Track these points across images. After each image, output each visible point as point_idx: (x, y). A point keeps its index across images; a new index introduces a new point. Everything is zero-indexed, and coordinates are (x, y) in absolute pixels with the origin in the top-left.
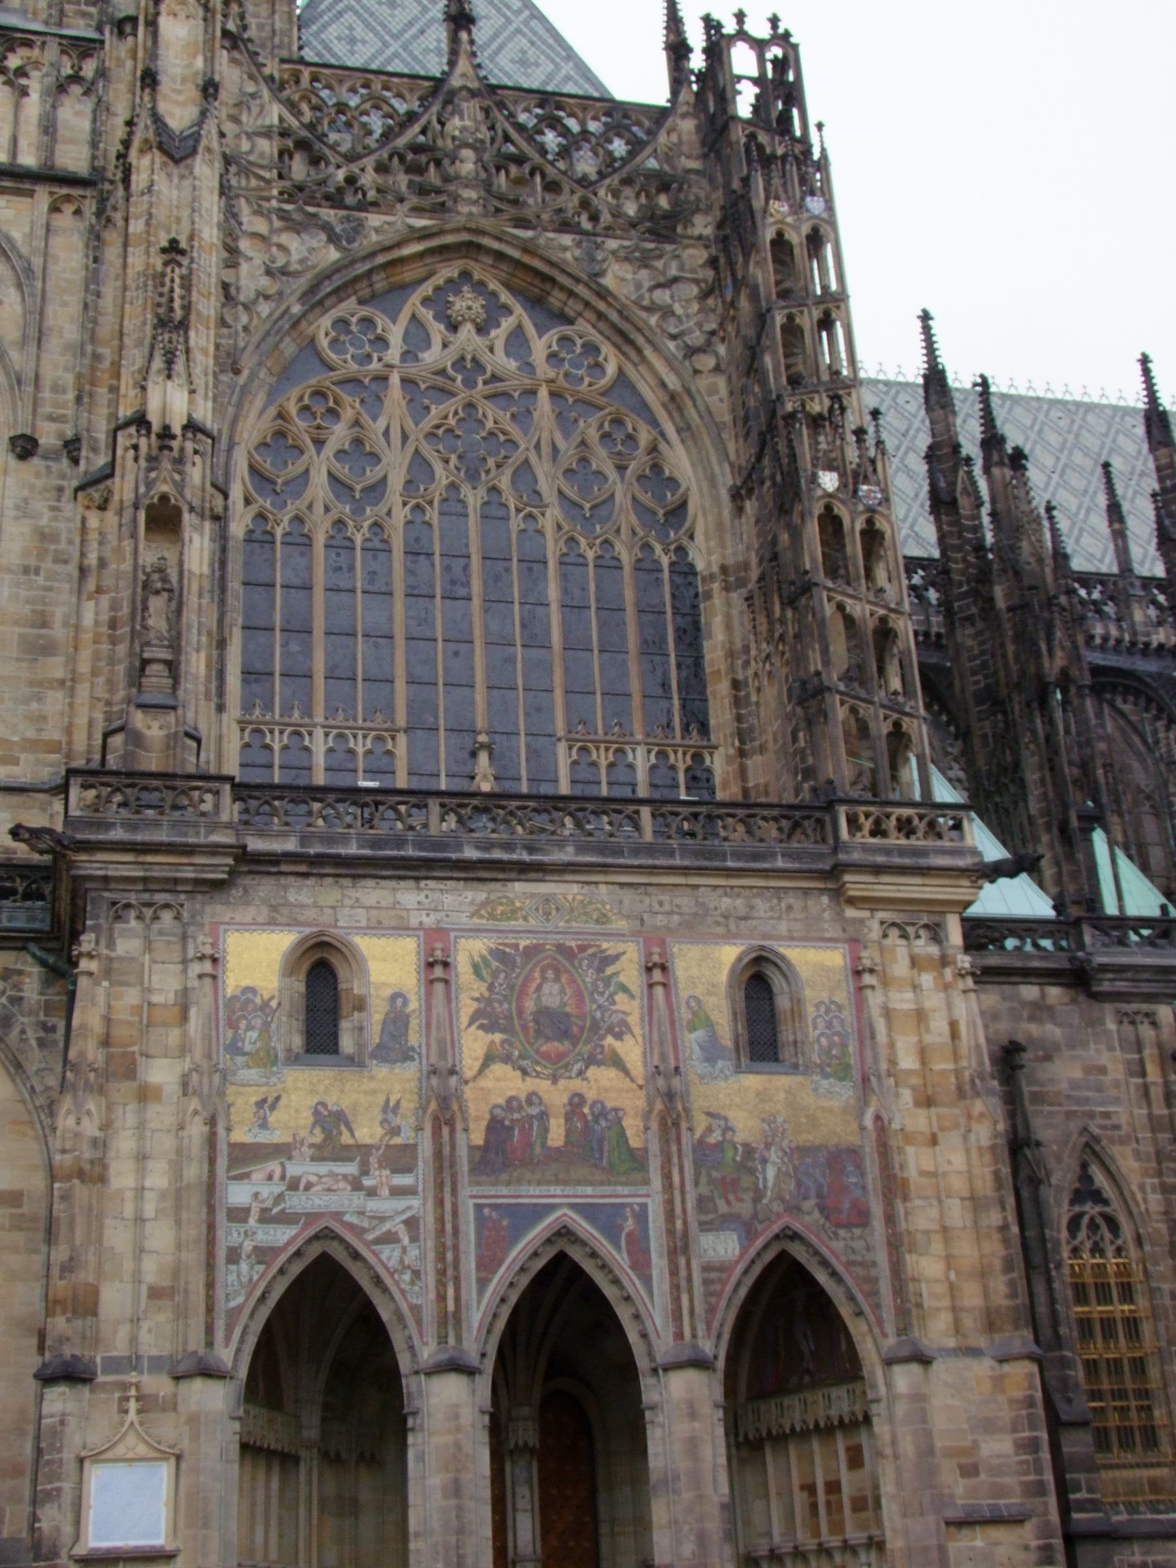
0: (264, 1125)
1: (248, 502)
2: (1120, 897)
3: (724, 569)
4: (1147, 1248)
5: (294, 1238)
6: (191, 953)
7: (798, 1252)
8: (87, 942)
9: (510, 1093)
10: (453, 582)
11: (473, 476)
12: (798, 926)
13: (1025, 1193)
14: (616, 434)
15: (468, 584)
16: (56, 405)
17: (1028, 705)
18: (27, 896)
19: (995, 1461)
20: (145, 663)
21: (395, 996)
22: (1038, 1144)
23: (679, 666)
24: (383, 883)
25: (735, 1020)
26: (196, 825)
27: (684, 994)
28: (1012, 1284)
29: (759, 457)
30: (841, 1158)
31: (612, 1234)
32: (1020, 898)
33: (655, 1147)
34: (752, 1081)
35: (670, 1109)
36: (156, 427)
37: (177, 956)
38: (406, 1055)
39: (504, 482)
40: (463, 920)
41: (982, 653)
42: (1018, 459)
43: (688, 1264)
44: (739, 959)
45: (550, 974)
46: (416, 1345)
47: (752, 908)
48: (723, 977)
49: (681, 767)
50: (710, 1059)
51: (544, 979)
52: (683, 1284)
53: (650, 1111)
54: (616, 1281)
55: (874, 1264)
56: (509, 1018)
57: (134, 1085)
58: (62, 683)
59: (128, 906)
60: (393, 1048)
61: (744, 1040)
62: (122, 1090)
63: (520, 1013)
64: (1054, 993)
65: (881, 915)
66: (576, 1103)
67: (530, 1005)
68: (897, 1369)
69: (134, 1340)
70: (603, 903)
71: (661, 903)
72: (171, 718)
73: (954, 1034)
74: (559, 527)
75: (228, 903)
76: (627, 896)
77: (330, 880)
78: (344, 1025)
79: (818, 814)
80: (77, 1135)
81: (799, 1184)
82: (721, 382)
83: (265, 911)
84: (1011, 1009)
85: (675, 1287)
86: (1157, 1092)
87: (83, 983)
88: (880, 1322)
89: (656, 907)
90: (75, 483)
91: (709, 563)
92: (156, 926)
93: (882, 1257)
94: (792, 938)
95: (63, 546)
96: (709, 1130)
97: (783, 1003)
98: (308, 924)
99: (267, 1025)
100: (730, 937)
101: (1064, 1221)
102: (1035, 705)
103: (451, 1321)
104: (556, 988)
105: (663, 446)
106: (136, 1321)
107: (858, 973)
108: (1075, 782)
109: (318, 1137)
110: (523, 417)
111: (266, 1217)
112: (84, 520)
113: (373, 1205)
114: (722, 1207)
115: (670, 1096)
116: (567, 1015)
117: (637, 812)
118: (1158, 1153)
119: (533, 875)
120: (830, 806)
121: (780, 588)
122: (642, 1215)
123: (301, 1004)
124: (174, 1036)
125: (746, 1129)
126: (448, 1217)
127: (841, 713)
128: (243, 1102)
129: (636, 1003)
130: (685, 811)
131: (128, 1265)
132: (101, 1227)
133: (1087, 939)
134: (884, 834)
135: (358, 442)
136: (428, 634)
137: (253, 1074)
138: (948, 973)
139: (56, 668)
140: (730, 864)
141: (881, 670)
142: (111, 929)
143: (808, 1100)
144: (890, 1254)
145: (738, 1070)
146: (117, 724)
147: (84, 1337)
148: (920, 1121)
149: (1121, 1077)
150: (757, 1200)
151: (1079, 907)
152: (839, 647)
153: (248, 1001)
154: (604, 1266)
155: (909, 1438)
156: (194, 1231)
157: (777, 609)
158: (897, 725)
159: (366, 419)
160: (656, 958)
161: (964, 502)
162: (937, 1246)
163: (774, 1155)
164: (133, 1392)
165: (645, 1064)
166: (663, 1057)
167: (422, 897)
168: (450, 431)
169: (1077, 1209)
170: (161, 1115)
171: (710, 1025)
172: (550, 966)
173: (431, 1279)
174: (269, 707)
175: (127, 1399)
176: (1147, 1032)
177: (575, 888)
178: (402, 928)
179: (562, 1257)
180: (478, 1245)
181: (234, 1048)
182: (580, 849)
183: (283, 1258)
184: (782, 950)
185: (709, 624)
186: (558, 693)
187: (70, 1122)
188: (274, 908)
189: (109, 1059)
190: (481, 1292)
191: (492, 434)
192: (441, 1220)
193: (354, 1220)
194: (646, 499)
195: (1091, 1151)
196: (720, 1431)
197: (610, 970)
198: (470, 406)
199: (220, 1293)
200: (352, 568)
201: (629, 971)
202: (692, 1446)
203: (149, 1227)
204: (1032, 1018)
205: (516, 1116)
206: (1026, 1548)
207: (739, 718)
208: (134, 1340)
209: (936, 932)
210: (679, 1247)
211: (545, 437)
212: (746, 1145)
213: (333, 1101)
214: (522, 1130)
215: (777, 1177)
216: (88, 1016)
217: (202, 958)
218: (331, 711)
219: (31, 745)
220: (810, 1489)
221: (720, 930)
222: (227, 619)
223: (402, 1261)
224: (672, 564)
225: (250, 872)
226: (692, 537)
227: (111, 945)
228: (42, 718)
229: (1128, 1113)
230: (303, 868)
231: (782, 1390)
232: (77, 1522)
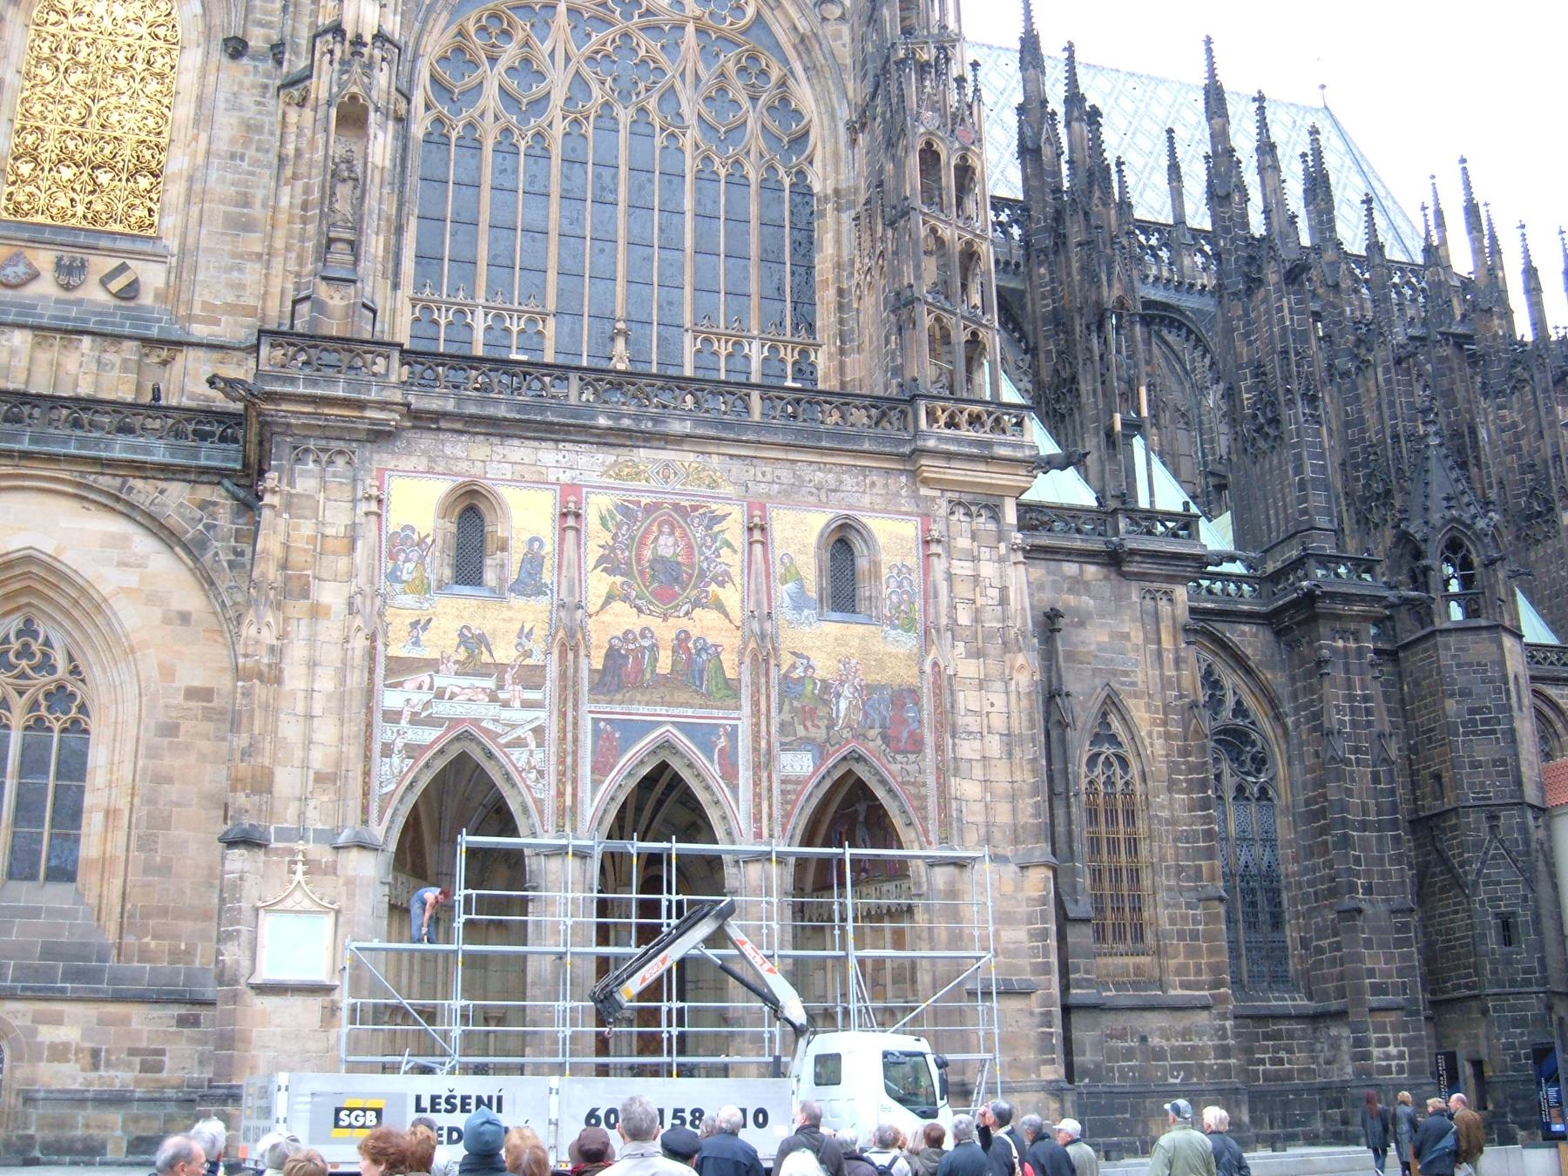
0: (416, 643)
1: (428, 108)
2: (1152, 494)
3: (837, 192)
4: (1150, 783)
5: (439, 738)
6: (360, 494)
7: (862, 772)
8: (271, 479)
10: (603, 189)
11: (625, 96)
12: (879, 500)
13: (1054, 734)
14: (751, 67)
15: (615, 191)
16: (265, 12)
17: (1088, 328)
18: (223, 439)
19: (1012, 946)
20: (331, 241)
22: (1068, 695)
23: (793, 273)
24: (527, 443)
25: (821, 576)
26: (369, 384)
27: (779, 552)
28: (1037, 805)
29: (873, 97)
30: (904, 697)
31: (707, 749)
32: (1067, 489)
33: (746, 678)
35: (762, 651)
36: (350, 35)
37: (347, 495)
38: (539, 590)
39: (652, 104)
40: (595, 479)
41: (1052, 280)
42: (1094, 116)
43: (770, 777)
44: (828, 525)
45: (666, 529)
47: (841, 482)
48: (813, 540)
49: (790, 360)
50: (798, 608)
51: (661, 532)
52: (764, 793)
53: (745, 648)
54: (708, 788)
55: (924, 784)
56: (629, 564)
57: (308, 602)
58: (260, 256)
59: (307, 450)
60: (528, 584)
61: (828, 591)
62: (297, 607)
63: (639, 561)
64: (1091, 570)
65: (949, 494)
66: (682, 638)
67: (648, 554)
68: (937, 870)
69: (301, 815)
71: (764, 474)
72: (351, 290)
73: (1003, 601)
74: (697, 147)
75: (393, 453)
76: (736, 466)
77: (482, 438)
78: (488, 561)
79: (902, 407)
80: (257, 642)
81: (866, 715)
82: (845, 30)
83: (424, 461)
84: (1054, 582)
85: (757, 795)
86: (1169, 657)
87: (267, 514)
88: (926, 832)
89: (759, 477)
90: (278, 82)
91: (825, 187)
93: (931, 780)
94: (874, 510)
95: (265, 137)
96: (794, 666)
97: (862, 564)
99: (422, 558)
100: (821, 505)
101: (1085, 759)
102: (1093, 327)
103: (568, 813)
104: (671, 541)
105: (791, 82)
106: (303, 800)
107: (927, 543)
108: (1121, 395)
109: (462, 655)
110: (672, 48)
111: (415, 720)
112: (284, 114)
113: (506, 715)
114: (801, 732)
115: (763, 636)
116: (678, 563)
117: (748, 395)
118: (1166, 706)
119: (656, 444)
120: (914, 398)
121: (885, 211)
122: (733, 735)
123: (453, 542)
124: (343, 563)
125: (824, 667)
126: (569, 728)
127: (928, 321)
128: (399, 623)
129: (738, 557)
130: (788, 396)
131: (299, 754)
132: (277, 719)
133: (1122, 526)
134: (957, 427)
135: (527, 61)
136: (579, 233)
137: (409, 599)
138: (1002, 546)
139: (255, 243)
140: (824, 444)
141: (964, 286)
142: (292, 470)
143: (878, 647)
144: (938, 778)
145: (821, 618)
146: (302, 295)
147: (260, 811)
148: (969, 669)
149: (1140, 642)
150: (829, 728)
151: (1118, 502)
152: (930, 266)
153: (407, 537)
156: (354, 728)
157: (880, 228)
158: (974, 334)
159: (535, 40)
160: (757, 520)
161: (1047, 151)
162: (978, 772)
163: (847, 691)
164: (300, 857)
165: (742, 609)
166: (758, 603)
167: (560, 457)
168: (607, 56)
169: (1096, 750)
170: (330, 630)
171: (800, 580)
172: (665, 522)
173: (553, 778)
174: (437, 287)
175: (295, 863)
176: (1164, 607)
177: (692, 456)
178: (541, 483)
179: (664, 766)
180: (594, 752)
181: (393, 577)
182: (698, 422)
184: (863, 520)
185: (821, 239)
186: (688, 290)
187: (253, 631)
188: (432, 460)
189: (287, 579)
190: (594, 792)
191: (643, 61)
192: (563, 730)
193: (491, 726)
194: (774, 126)
195: (1112, 703)
197: (716, 528)
198: (626, 35)
199: (375, 783)
200: (515, 171)
201: (733, 529)
203: (316, 722)
204: (1070, 591)
205: (631, 646)
206: (1031, 1013)
207: (841, 322)
208: (301, 815)
209: (995, 512)
210: (764, 763)
211: (690, 66)
212: (823, 681)
213: (477, 626)
214: (636, 658)
215: (848, 709)
216: (269, 542)
217: (369, 498)
218: (492, 292)
219: (231, 309)
221: (812, 499)
222: (405, 210)
223: (529, 762)
224: (792, 185)
225: (414, 427)
226: (811, 163)
227: (291, 484)
228: (241, 286)
229: (1144, 674)
230: (459, 426)
232: (253, 959)
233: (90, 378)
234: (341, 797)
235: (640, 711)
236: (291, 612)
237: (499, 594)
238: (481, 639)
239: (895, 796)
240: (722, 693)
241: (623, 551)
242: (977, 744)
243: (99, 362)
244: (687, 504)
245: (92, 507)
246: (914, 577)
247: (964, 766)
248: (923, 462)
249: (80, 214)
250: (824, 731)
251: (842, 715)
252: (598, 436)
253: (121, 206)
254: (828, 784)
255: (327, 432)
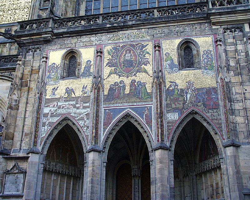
0: (54, 94)
7: (198, 118)
9: (115, 81)
21: (88, 61)
24: (87, 36)
27: (164, 53)
30: (210, 91)
31: (141, 115)
33: (154, 91)
34: (184, 72)
43: (162, 122)
44: (181, 42)
45: (128, 52)
46: (87, 145)
51: (126, 53)
54: (142, 127)
55: (221, 119)
59: (30, 49)
60: (87, 73)
65: (223, 26)
68: (227, 148)
69: (21, 145)
70: (143, 34)
71: (159, 31)
75: (51, 45)
76: (150, 31)
78: (77, 69)
83: (59, 46)
88: (222, 135)
92: (35, 53)
94: (196, 35)
96: (171, 86)
97: (195, 52)
98: (67, 48)
104: (129, 55)
113: (78, 111)
117: (153, 11)
119: (125, 29)
125: (181, 85)
128: (49, 88)
129: (151, 56)
131: (21, 128)
138: (245, 39)
142: (26, 54)
145: (180, 70)
148: (235, 79)
150: (184, 104)
154: (139, 124)
155: (231, 169)
162: (242, 113)
170: (31, 95)
171: (172, 60)
172: (128, 50)
177: (136, 31)
178: (91, 46)
181: (49, 77)
183: (56, 124)
184: (193, 39)
190: (104, 132)
196: (172, 167)
197: (144, 49)
201: (150, 48)
202: (161, 170)
208: (21, 145)
215: (190, 97)
217: (43, 58)
220: (212, 186)
223: (84, 124)
227: (25, 58)
230: (69, 35)
231: (206, 159)
233: (8, 52)
234: (30, 139)
235: (118, 106)
236: (23, 91)
237: (78, 77)
238: (72, 90)
239: (210, 124)
240: (146, 97)
241: (114, 60)
242: (241, 104)
243: (10, 49)
244: (135, 44)
245: (5, 81)
246: (212, 53)
247: (237, 112)
248: (211, 18)
249: (12, 20)
250: (182, 105)
251: (188, 99)
252: (107, 30)
253: (20, 16)
254: (185, 123)
255: (34, 43)
